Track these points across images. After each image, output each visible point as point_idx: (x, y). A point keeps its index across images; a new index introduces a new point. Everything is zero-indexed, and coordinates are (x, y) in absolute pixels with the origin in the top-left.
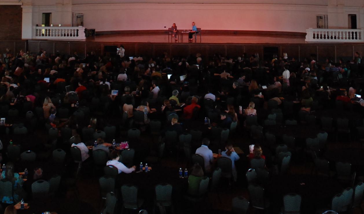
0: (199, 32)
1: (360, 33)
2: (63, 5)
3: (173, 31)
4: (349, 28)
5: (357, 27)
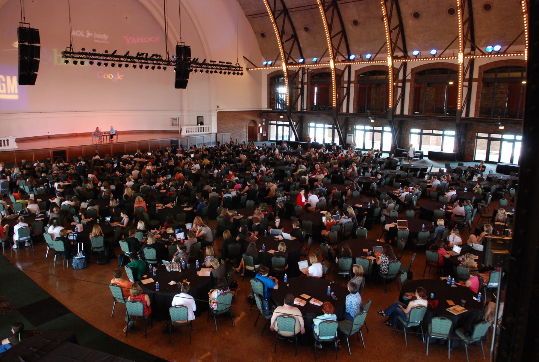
0: (117, 133)
1: (208, 127)
3: (97, 133)
5: (204, 124)
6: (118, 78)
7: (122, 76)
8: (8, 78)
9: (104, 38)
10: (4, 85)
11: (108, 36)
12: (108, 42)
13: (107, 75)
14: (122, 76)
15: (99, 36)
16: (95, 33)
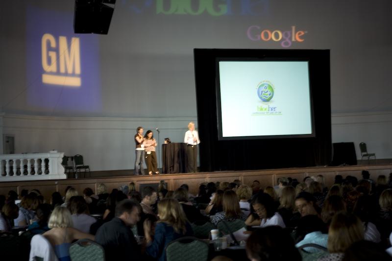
6: (293, 40)
8: (63, 40)
10: (53, 55)
13: (269, 32)
14: (303, 33)
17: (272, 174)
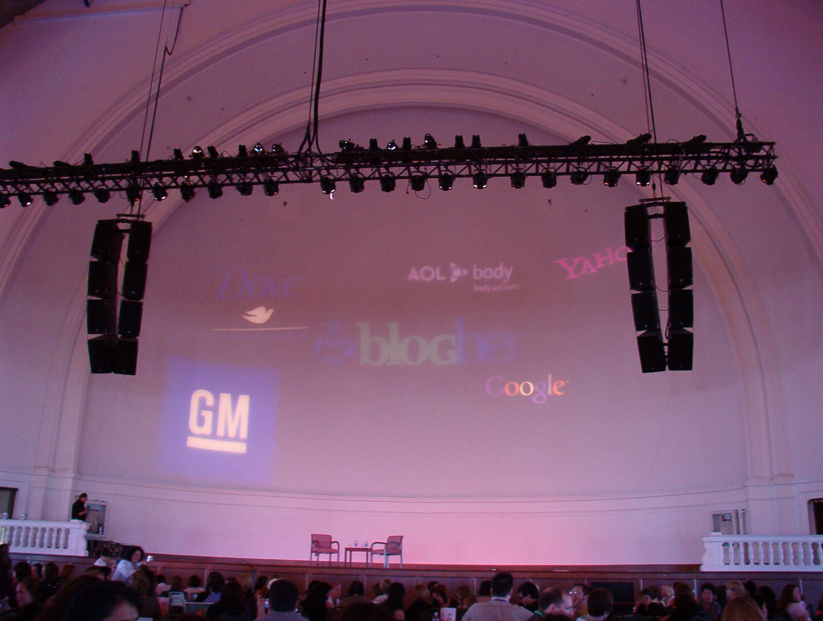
2: (53, 471)
4: (811, 534)
6: (550, 393)
7: (563, 383)
8: (225, 399)
9: (501, 276)
11: (511, 269)
12: (512, 287)
13: (517, 385)
14: (563, 383)
15: (488, 274)
16: (475, 266)
17: (204, 569)
